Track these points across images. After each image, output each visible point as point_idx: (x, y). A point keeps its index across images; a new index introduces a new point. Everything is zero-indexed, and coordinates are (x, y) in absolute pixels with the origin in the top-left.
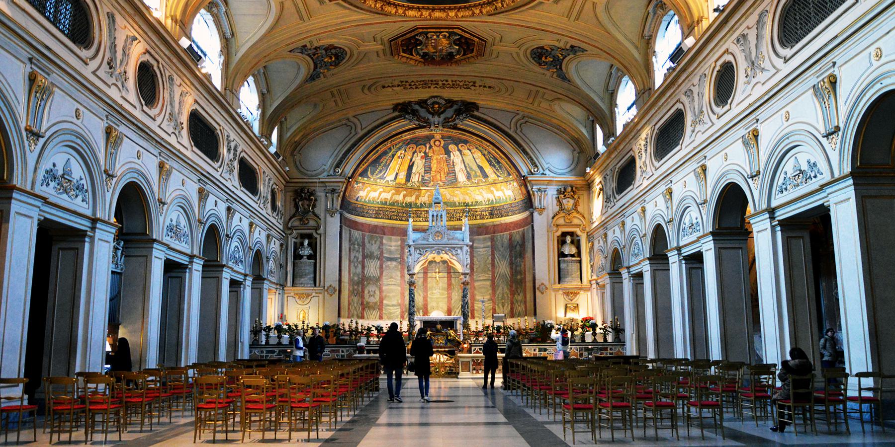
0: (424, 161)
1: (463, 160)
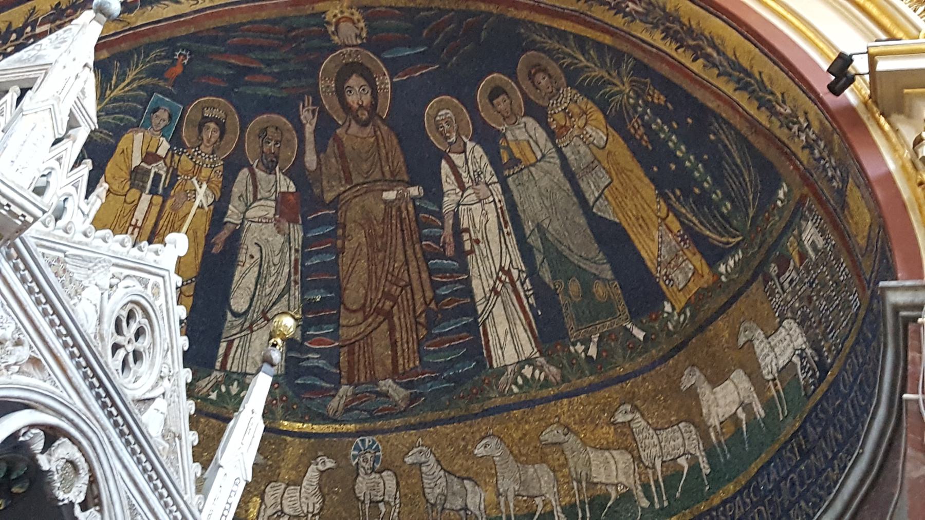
0: (297, 233)
1: (512, 206)
